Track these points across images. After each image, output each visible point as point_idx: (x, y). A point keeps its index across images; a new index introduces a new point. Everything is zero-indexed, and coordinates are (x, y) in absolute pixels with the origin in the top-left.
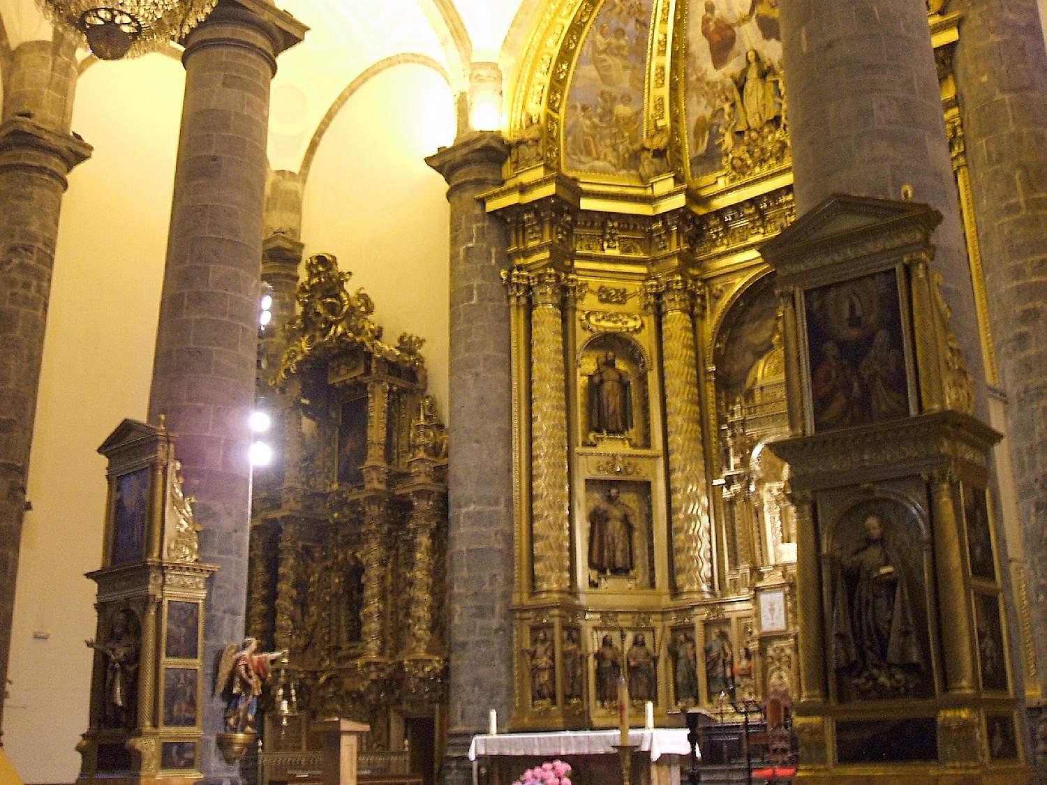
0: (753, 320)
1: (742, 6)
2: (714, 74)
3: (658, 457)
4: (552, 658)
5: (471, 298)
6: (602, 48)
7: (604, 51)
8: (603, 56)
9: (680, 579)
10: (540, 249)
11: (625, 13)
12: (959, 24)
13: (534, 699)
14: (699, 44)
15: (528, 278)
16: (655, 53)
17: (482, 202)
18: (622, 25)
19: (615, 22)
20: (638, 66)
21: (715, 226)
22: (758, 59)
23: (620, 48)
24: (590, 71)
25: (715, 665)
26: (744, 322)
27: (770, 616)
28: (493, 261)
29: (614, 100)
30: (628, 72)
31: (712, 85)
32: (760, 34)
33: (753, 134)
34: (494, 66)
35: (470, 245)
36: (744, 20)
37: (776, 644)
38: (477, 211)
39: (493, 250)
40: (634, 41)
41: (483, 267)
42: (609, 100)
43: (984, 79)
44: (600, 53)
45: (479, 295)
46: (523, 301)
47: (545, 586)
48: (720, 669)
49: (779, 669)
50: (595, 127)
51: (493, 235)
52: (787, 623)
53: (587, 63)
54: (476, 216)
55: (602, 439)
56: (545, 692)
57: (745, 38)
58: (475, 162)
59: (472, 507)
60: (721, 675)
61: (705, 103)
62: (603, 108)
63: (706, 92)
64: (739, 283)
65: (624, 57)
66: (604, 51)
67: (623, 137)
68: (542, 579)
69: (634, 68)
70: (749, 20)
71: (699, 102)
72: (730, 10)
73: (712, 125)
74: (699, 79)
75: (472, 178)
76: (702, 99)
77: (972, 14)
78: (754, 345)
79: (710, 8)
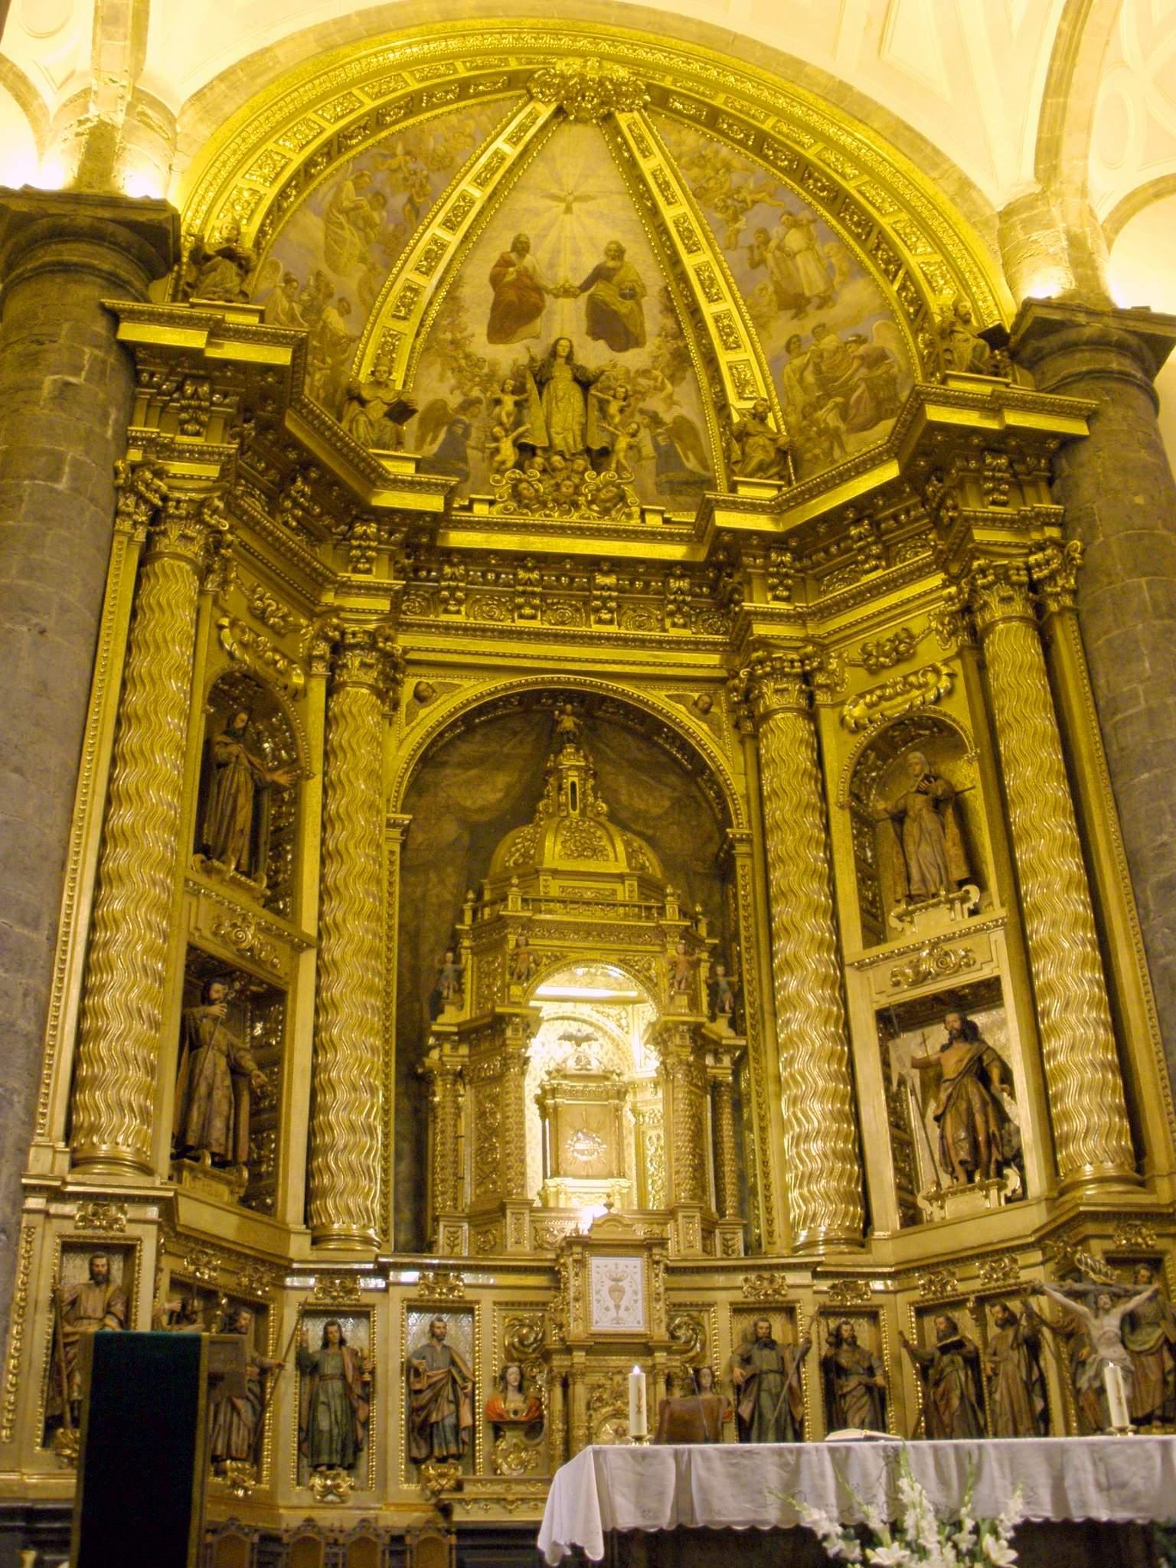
0: (465, 765)
1: (574, 270)
2: (480, 345)
3: (309, 946)
6: (346, 204)
8: (342, 219)
11: (400, 176)
12: (1090, 417)
14: (478, 296)
15: (165, 499)
16: (410, 265)
18: (387, 191)
20: (380, 268)
21: (453, 578)
22: (569, 358)
23: (369, 223)
24: (313, 226)
26: (444, 764)
27: (611, 1304)
28: (110, 433)
29: (330, 295)
30: (363, 267)
31: (479, 363)
32: (584, 325)
33: (556, 459)
34: (172, 120)
35: (72, 380)
36: (566, 292)
39: (113, 415)
40: (391, 227)
41: (90, 432)
43: (1139, 500)
44: (340, 212)
46: (141, 536)
51: (118, 384)
52: (650, 1320)
53: (318, 214)
54: (96, 335)
55: (219, 872)
57: (557, 317)
58: (115, 245)
60: (450, 1421)
61: (453, 382)
62: (313, 299)
63: (460, 370)
64: (472, 689)
65: (368, 241)
67: (323, 361)
69: (372, 269)
70: (575, 296)
71: (442, 378)
72: (552, 266)
73: (455, 422)
75: (106, 267)
76: (449, 374)
78: (465, 809)
79: (521, 247)
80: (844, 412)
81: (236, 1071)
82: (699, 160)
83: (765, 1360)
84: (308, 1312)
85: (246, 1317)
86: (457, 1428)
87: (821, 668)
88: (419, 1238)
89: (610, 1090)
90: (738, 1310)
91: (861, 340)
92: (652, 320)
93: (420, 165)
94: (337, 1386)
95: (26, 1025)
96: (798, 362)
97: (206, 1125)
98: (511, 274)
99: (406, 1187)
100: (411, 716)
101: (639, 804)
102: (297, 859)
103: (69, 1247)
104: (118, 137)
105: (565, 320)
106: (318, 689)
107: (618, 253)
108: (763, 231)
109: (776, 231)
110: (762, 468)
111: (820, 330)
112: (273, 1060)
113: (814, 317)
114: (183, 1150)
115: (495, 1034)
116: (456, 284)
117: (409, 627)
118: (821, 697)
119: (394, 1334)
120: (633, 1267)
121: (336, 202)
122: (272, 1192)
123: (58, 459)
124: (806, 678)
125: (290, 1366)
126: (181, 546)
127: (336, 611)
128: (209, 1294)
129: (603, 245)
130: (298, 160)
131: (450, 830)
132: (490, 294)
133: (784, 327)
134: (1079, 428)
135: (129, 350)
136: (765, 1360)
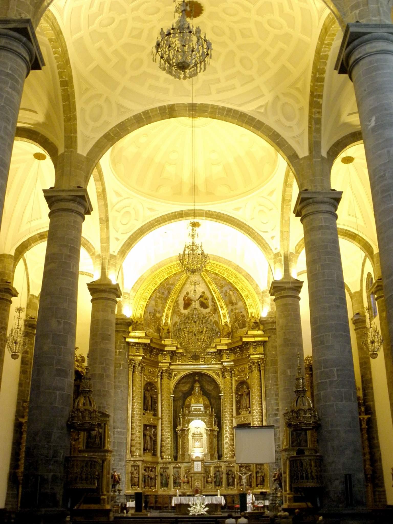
0: (183, 383)
2: (183, 311)
4: (139, 474)
5: (120, 367)
7: (158, 298)
9: (163, 454)
10: (139, 356)
12: (269, 337)
13: (132, 486)
17: (125, 338)
19: (163, 291)
23: (162, 298)
25: (176, 479)
31: (182, 314)
34: (129, 294)
37: (197, 475)
38: (123, 340)
42: (156, 311)
43: (274, 353)
45: (123, 366)
46: (132, 370)
47: (135, 454)
48: (178, 480)
49: (198, 481)
50: (151, 319)
56: (136, 484)
59: (119, 430)
64: (183, 374)
66: (158, 298)
68: (134, 452)
71: (177, 317)
74: (178, 311)
77: (273, 336)
80: (239, 324)
81: (151, 438)
82: (215, 279)
83: (218, 473)
84: (161, 468)
85: (153, 470)
86: (179, 483)
87: (233, 370)
88: (176, 458)
89: (201, 435)
90: (215, 467)
91: (241, 312)
92: (210, 303)
93: (169, 286)
94: (164, 477)
95: (125, 441)
96: (233, 313)
97: (147, 446)
98: (186, 298)
99: (175, 447)
100: (174, 378)
101: (208, 388)
102: (158, 406)
103: (132, 466)
104: (122, 303)
105: (196, 305)
106: (159, 379)
107: (204, 293)
108: (226, 291)
109: (228, 291)
110: (225, 335)
111: (236, 309)
112: (155, 435)
113: (235, 306)
114: (145, 450)
115: (185, 431)
116: (178, 301)
117: (173, 365)
118: (233, 375)
119: (171, 471)
120: (200, 463)
121: (156, 297)
122: (156, 452)
123: (120, 364)
124: (231, 372)
125: (159, 475)
126: (138, 369)
127: (161, 367)
128: (149, 467)
129: (201, 292)
130: (149, 296)
131: (181, 394)
132: (183, 302)
133: (230, 307)
134: (267, 339)
135: (128, 343)
136: (218, 473)
